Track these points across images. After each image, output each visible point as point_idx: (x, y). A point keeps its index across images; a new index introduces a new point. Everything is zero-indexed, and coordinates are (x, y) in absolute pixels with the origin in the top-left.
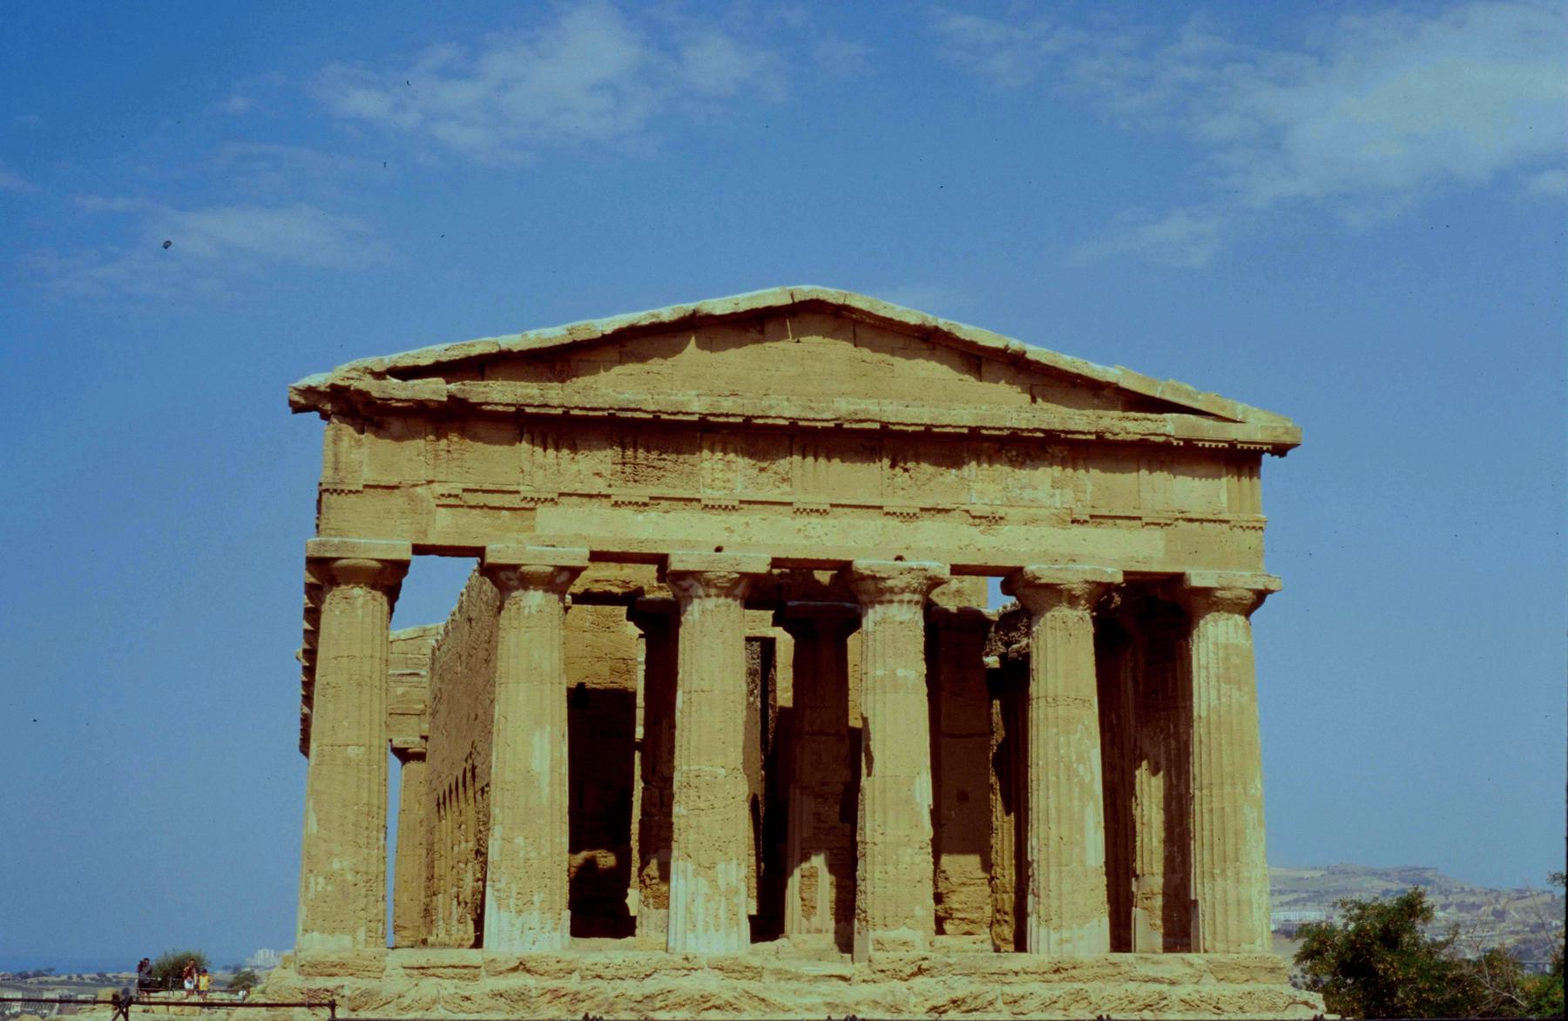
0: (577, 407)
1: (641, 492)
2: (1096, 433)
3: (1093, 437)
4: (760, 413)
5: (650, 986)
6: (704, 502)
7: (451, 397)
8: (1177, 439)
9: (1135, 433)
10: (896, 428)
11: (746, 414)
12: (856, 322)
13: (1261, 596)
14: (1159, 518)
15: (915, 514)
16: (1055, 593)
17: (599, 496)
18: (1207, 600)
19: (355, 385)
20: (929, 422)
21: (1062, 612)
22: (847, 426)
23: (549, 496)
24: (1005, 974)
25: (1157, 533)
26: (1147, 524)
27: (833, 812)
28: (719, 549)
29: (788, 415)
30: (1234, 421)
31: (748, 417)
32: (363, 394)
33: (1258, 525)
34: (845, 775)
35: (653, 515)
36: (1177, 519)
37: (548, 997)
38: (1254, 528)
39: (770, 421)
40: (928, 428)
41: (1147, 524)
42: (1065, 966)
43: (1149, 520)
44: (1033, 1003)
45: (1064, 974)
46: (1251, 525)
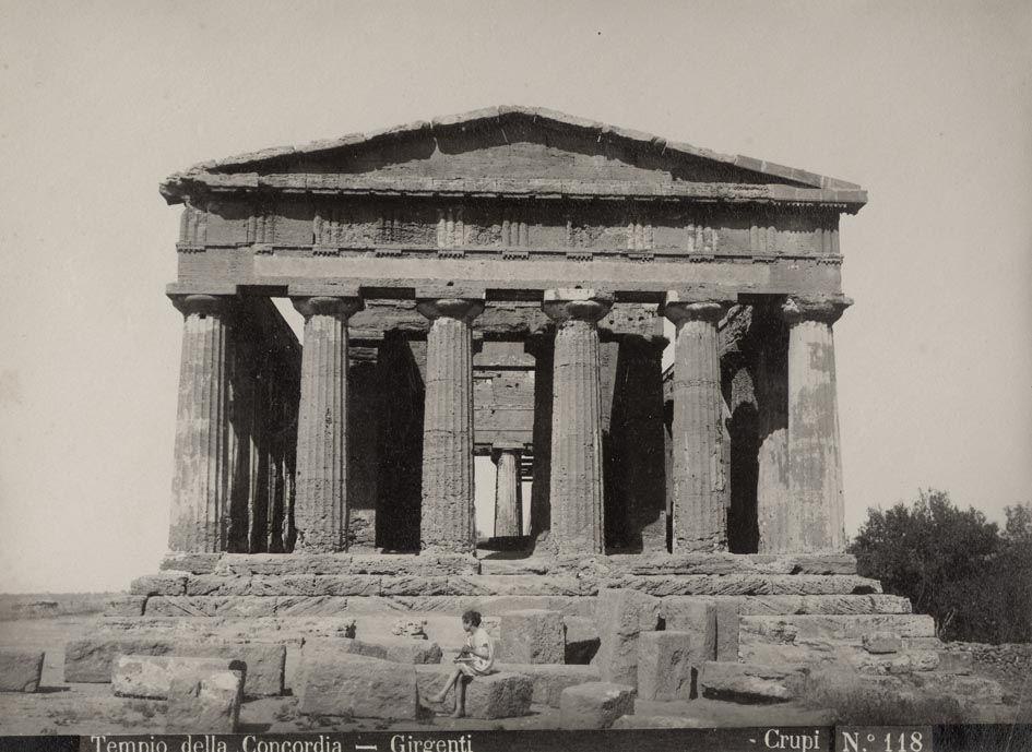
1: (397, 247)
4: (475, 190)
7: (261, 185)
17: (366, 250)
19: (197, 178)
25: (766, 269)
26: (757, 261)
28: (451, 284)
29: (495, 191)
32: (202, 184)
36: (778, 258)
41: (757, 261)
43: (757, 258)
46: (831, 260)
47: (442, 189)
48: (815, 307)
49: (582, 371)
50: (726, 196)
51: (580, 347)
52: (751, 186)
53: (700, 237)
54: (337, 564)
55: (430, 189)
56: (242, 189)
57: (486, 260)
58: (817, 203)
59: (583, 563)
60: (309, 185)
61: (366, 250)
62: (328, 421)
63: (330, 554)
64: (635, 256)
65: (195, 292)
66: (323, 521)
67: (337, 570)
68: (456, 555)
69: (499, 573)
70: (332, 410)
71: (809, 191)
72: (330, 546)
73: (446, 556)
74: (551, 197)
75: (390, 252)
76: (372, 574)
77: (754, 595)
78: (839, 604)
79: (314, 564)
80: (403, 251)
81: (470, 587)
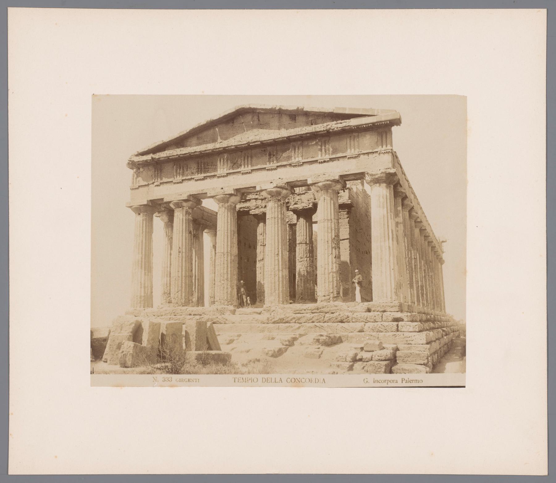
0: (181, 154)
2: (326, 130)
3: (326, 132)
4: (226, 146)
6: (217, 176)
7: (152, 158)
8: (353, 126)
9: (339, 128)
10: (265, 142)
11: (223, 147)
12: (259, 113)
14: (353, 155)
15: (275, 168)
20: (274, 138)
23: (179, 181)
24: (301, 310)
26: (348, 158)
29: (234, 145)
30: (374, 116)
31: (223, 148)
33: (388, 151)
36: (359, 154)
38: (387, 152)
42: (320, 307)
46: (385, 151)
47: (214, 148)
48: (377, 177)
49: (273, 221)
50: (330, 128)
51: (273, 210)
52: (343, 121)
53: (323, 150)
54: (182, 311)
55: (209, 149)
56: (146, 161)
57: (235, 176)
58: (373, 124)
59: (273, 308)
60: (168, 155)
61: (192, 179)
62: (179, 252)
63: (180, 308)
64: (294, 165)
65: (134, 205)
66: (177, 294)
67: (181, 314)
68: (224, 306)
69: (243, 314)
70: (181, 247)
71: (370, 118)
72: (180, 304)
73: (219, 307)
74: (256, 143)
75: (200, 178)
76: (194, 315)
77: (344, 322)
78: (380, 327)
79: (173, 312)
80: (204, 177)
81: (224, 320)
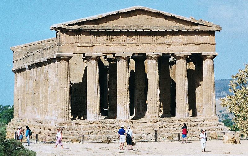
0: (100, 30)
1: (111, 43)
5: (115, 125)
7: (79, 29)
13: (215, 56)
16: (179, 58)
18: (205, 57)
21: (181, 60)
22: (145, 31)
27: (143, 93)
28: (124, 52)
34: (143, 87)
35: (112, 46)
37: (99, 127)
39: (132, 30)
40: (158, 30)
44: (177, 125)
45: (181, 121)
